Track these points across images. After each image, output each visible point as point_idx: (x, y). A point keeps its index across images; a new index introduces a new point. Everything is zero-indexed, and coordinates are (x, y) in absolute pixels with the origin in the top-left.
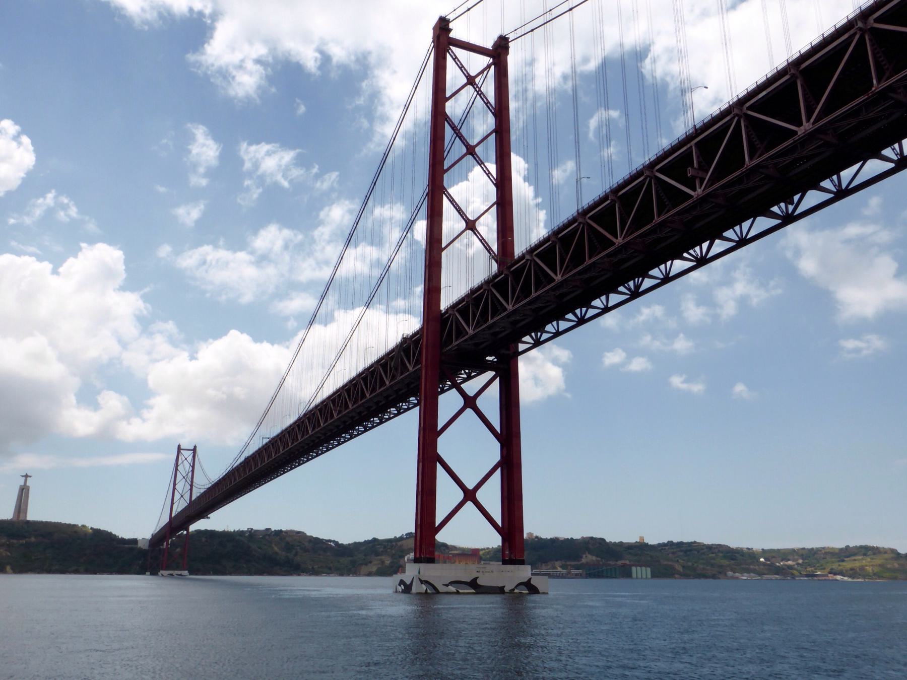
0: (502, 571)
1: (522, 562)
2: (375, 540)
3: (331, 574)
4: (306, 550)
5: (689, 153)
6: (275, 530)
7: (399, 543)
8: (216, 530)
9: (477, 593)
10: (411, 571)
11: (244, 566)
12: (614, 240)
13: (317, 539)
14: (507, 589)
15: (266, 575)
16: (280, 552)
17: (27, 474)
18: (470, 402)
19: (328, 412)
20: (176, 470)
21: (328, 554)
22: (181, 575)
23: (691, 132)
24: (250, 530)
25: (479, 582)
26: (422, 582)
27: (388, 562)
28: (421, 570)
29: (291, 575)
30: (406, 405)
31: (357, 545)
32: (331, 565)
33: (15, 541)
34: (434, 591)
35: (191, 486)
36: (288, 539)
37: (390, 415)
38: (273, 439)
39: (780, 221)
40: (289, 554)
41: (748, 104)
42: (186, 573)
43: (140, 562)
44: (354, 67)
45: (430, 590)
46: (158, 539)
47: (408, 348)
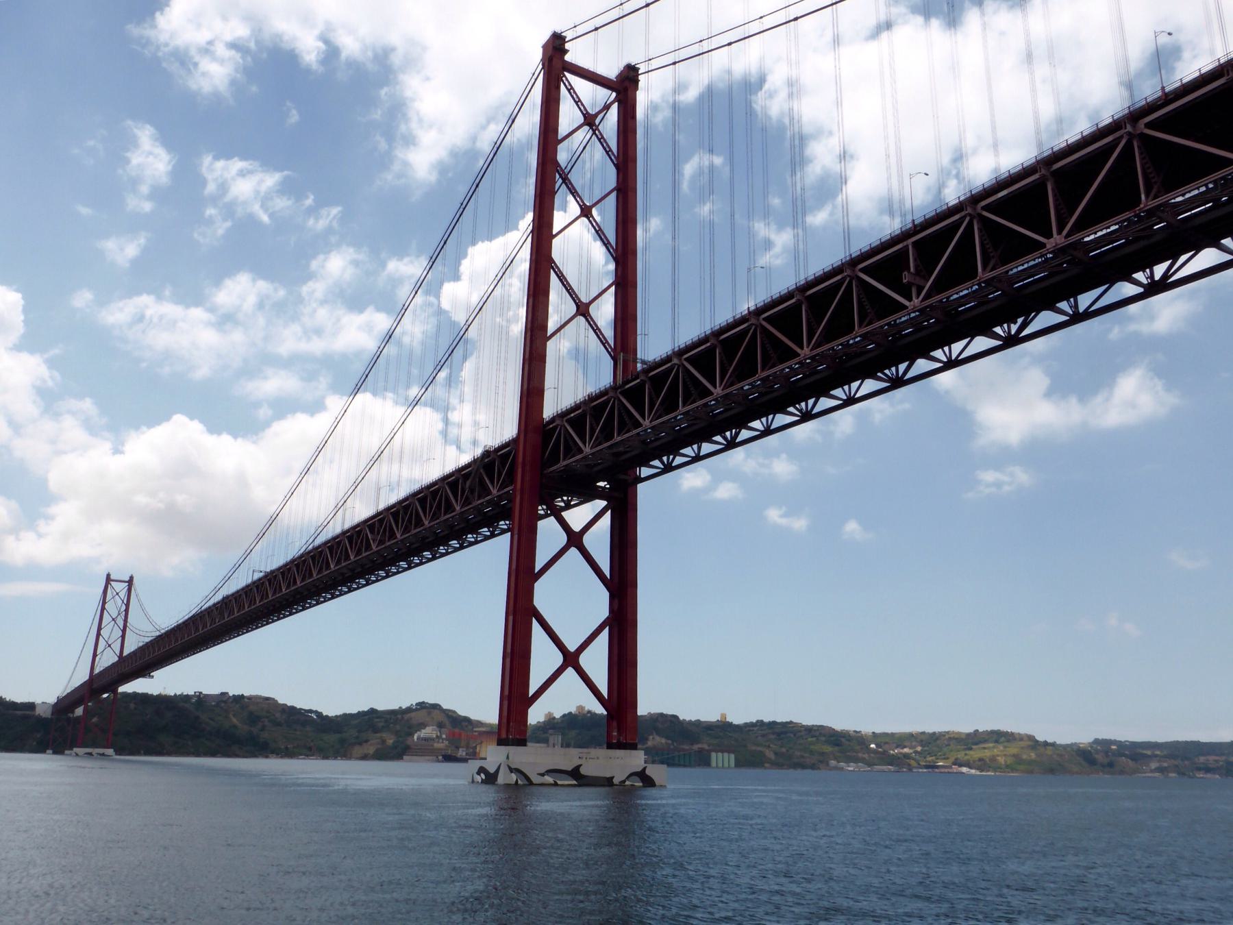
0: (610, 758)
1: (633, 747)
2: (372, 711)
5: (904, 252)
6: (234, 695)
7: (407, 716)
8: (149, 693)
9: (579, 785)
10: (494, 755)
11: (190, 743)
12: (799, 350)
13: (293, 708)
14: (616, 781)
18: (575, 539)
19: (362, 542)
20: (103, 609)
21: (308, 728)
22: (103, 755)
23: (908, 227)
24: (198, 694)
25: (583, 771)
26: (511, 770)
27: (390, 742)
28: (510, 755)
30: (473, 537)
31: (347, 717)
32: (312, 744)
34: (527, 783)
35: (124, 631)
36: (252, 708)
37: (448, 549)
38: (272, 572)
39: (1001, 343)
41: (983, 203)
42: (110, 751)
43: (39, 736)
46: (65, 705)
47: (492, 463)
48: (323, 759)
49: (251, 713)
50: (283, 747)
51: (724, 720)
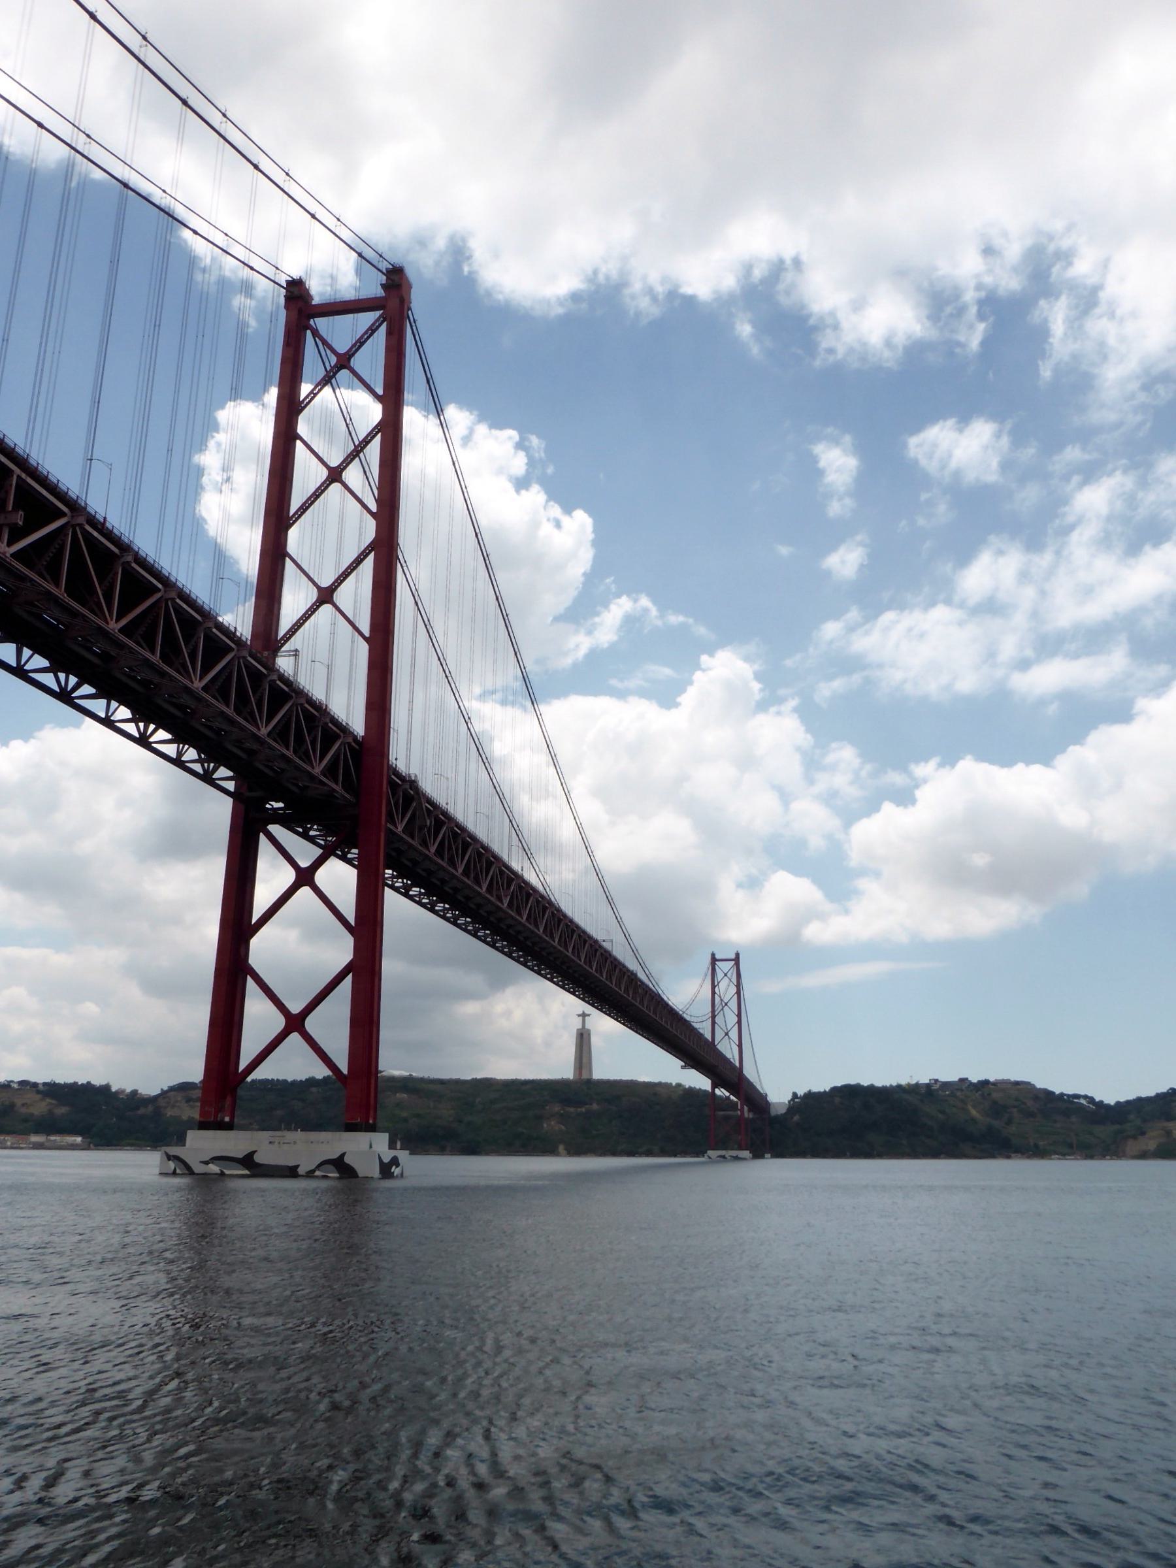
0: (312, 1142)
1: (372, 1129)
3: (1069, 1155)
14: (301, 1171)
15: (945, 1158)
17: (584, 1012)
18: (305, 877)
20: (713, 993)
21: (1074, 1119)
24: (933, 1082)
25: (258, 1158)
31: (1139, 1104)
33: (572, 1110)
34: (187, 1172)
36: (995, 1095)
42: (746, 1154)
44: (1058, 225)
45: (180, 1169)
48: (1085, 1159)
49: (995, 1103)
50: (1032, 1144)
51: (198, 1094)
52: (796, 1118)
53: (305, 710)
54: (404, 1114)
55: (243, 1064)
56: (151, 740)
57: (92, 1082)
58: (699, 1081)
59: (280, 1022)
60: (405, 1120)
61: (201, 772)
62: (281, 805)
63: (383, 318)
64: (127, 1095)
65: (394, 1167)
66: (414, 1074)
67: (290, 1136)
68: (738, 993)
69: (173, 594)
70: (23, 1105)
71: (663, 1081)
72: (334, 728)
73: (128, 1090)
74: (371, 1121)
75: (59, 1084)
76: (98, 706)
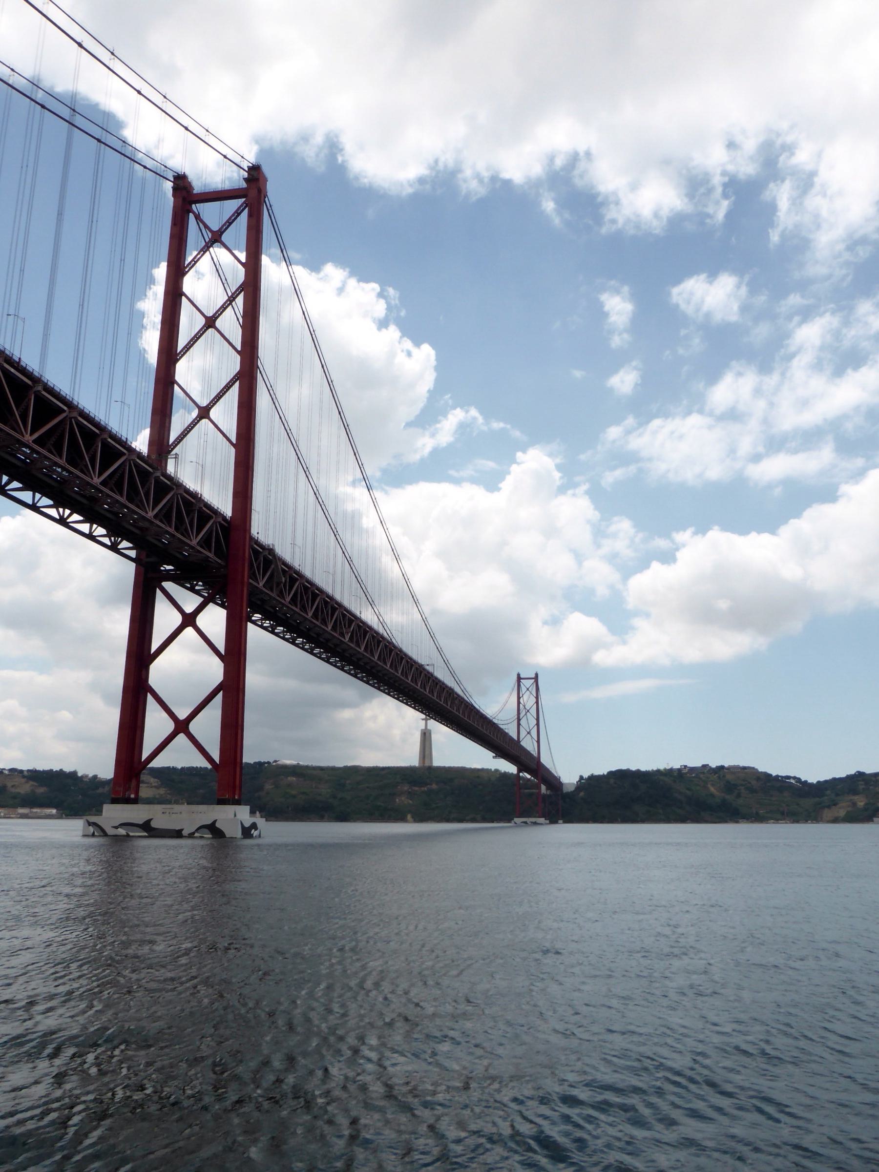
1: (238, 803)
2: (860, 775)
4: (752, 790)
9: (150, 837)
11: (661, 811)
14: (185, 833)
16: (718, 793)
20: (519, 703)
25: (154, 824)
27: (861, 804)
29: (725, 822)
33: (416, 789)
34: (102, 834)
36: (729, 777)
40: (727, 797)
42: (542, 820)
48: (793, 823)
49: (728, 782)
50: (754, 812)
52: (582, 794)
53: (183, 498)
54: (294, 792)
55: (145, 755)
56: (68, 520)
57: (64, 770)
58: (509, 768)
59: (170, 726)
60: (294, 796)
61: (109, 544)
62: (171, 567)
63: (246, 205)
64: (89, 779)
65: (253, 830)
66: (301, 763)
67: (177, 808)
68: (537, 702)
69: (75, 414)
70: (13, 786)
71: (485, 767)
72: (208, 512)
73: (91, 775)
74: (236, 797)
75: (39, 771)
76: (27, 496)
